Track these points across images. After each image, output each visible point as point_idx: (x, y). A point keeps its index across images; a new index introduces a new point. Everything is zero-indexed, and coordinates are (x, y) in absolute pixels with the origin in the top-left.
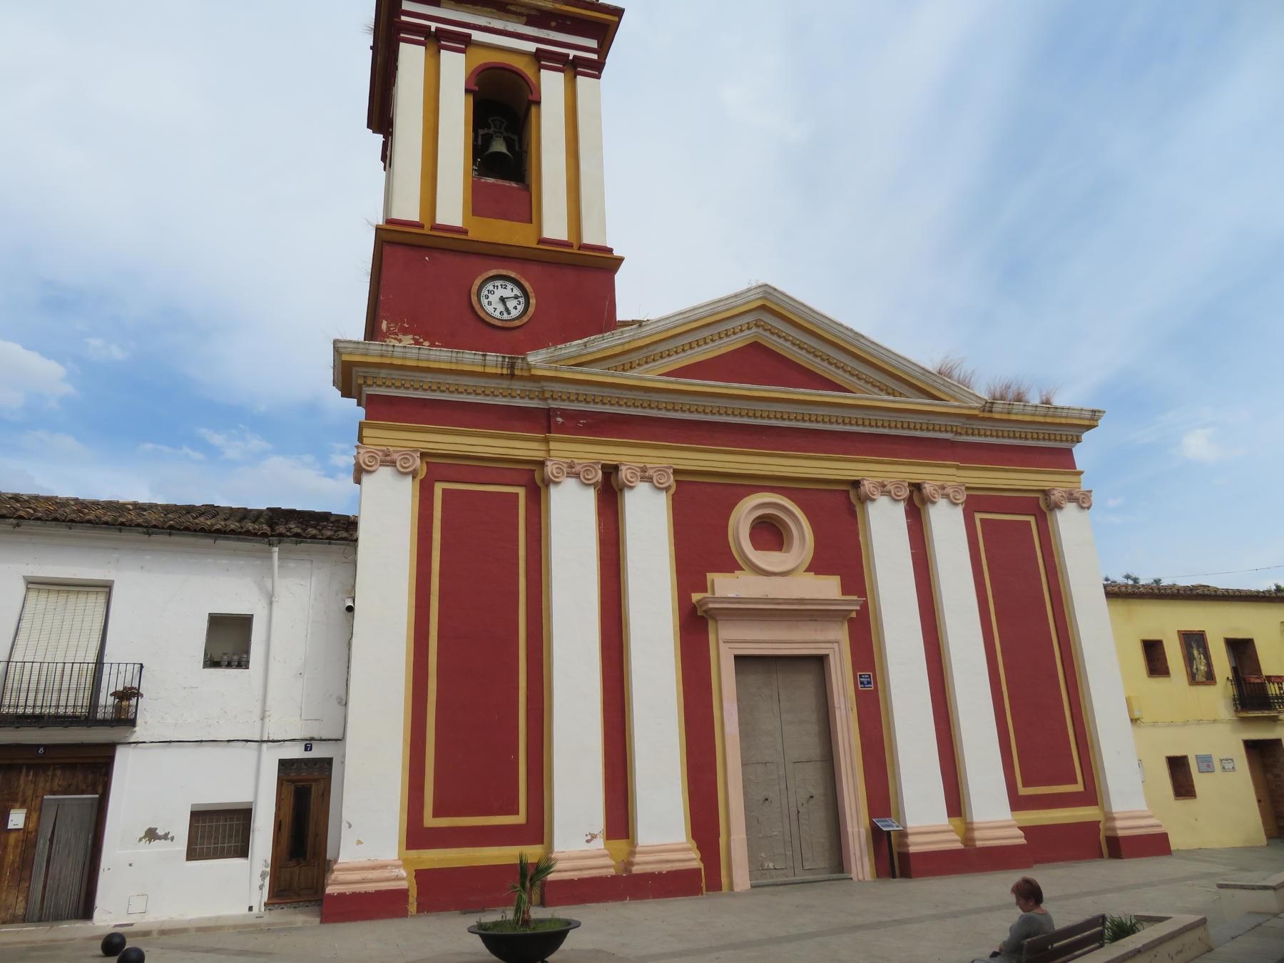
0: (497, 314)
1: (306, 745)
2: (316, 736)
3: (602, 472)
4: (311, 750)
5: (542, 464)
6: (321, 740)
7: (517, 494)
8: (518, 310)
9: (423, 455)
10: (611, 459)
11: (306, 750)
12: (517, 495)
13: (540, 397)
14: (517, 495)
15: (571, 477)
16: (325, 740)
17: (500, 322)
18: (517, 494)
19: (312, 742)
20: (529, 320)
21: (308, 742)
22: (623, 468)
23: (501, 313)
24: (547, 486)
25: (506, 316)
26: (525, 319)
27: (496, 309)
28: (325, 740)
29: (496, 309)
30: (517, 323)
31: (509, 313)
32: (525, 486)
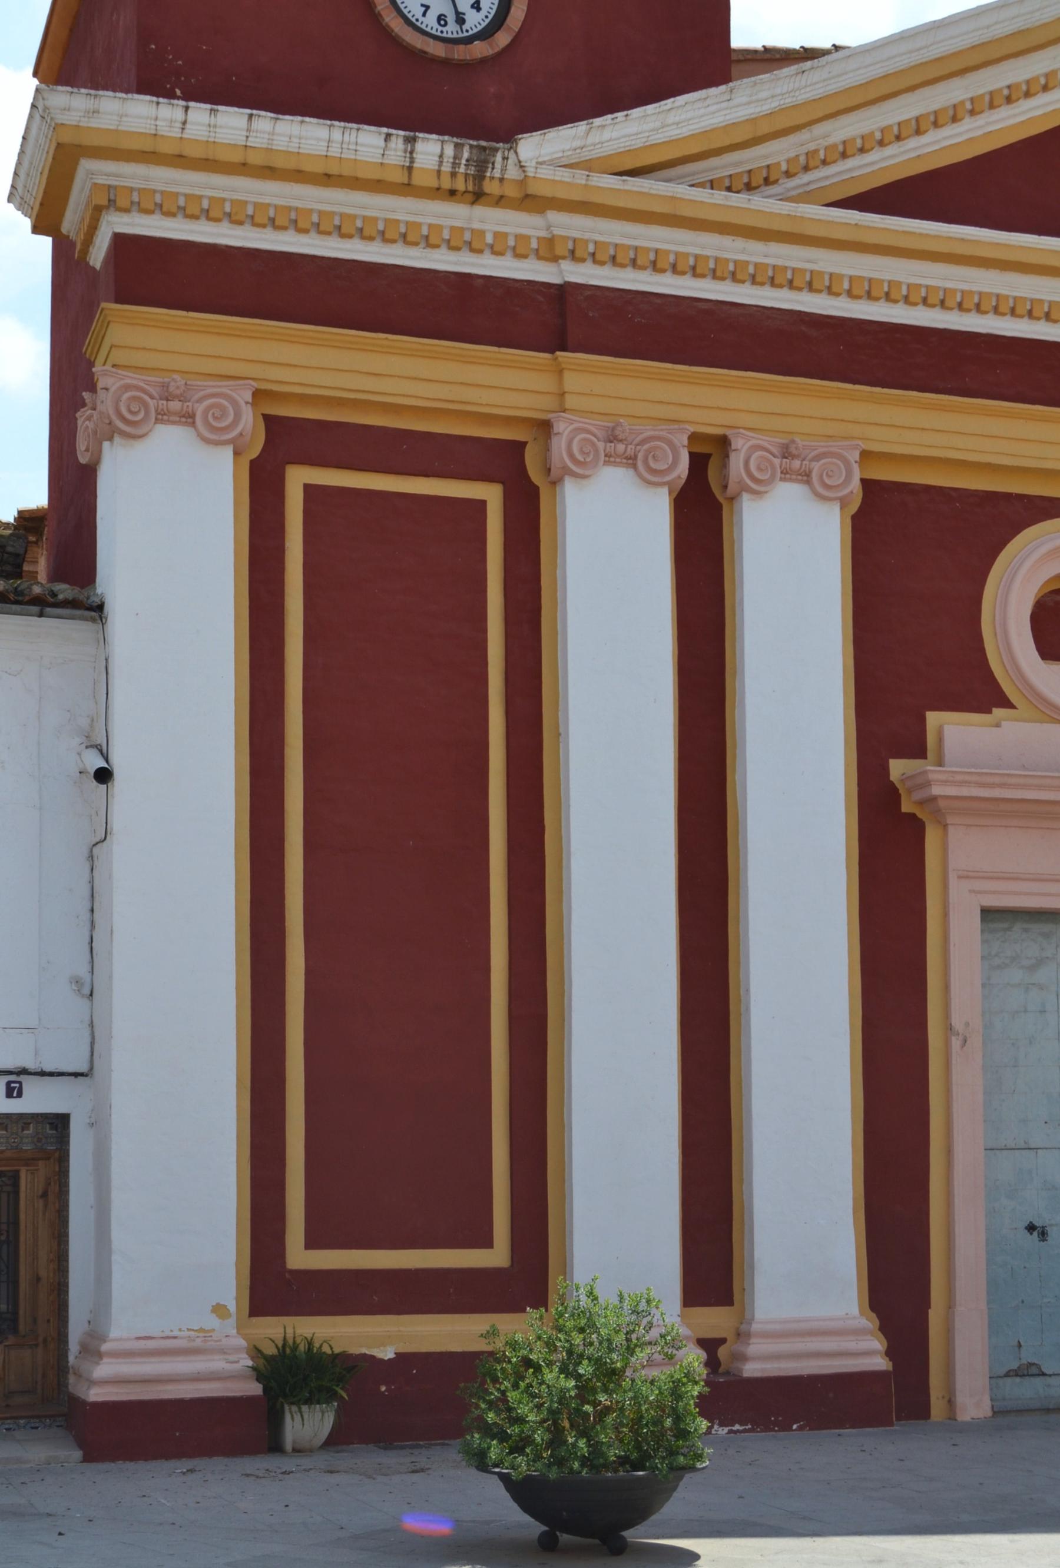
0: (430, 23)
1: (8, 1084)
2: (31, 1065)
3: (692, 455)
4: (20, 1095)
5: (544, 427)
6: (42, 1074)
7: (483, 503)
8: (483, 13)
9: (259, 395)
10: (710, 423)
11: (9, 1094)
12: (480, 506)
13: (541, 253)
14: (480, 506)
15: (615, 464)
16: (51, 1074)
17: (440, 44)
18: (483, 503)
19: (23, 1078)
20: (513, 41)
21: (13, 1078)
22: (740, 445)
23: (441, 19)
24: (555, 483)
25: (451, 30)
26: (503, 39)
27: (427, 7)
28: (51, 1074)
29: (427, 7)
30: (480, 50)
31: (460, 20)
32: (503, 483)
